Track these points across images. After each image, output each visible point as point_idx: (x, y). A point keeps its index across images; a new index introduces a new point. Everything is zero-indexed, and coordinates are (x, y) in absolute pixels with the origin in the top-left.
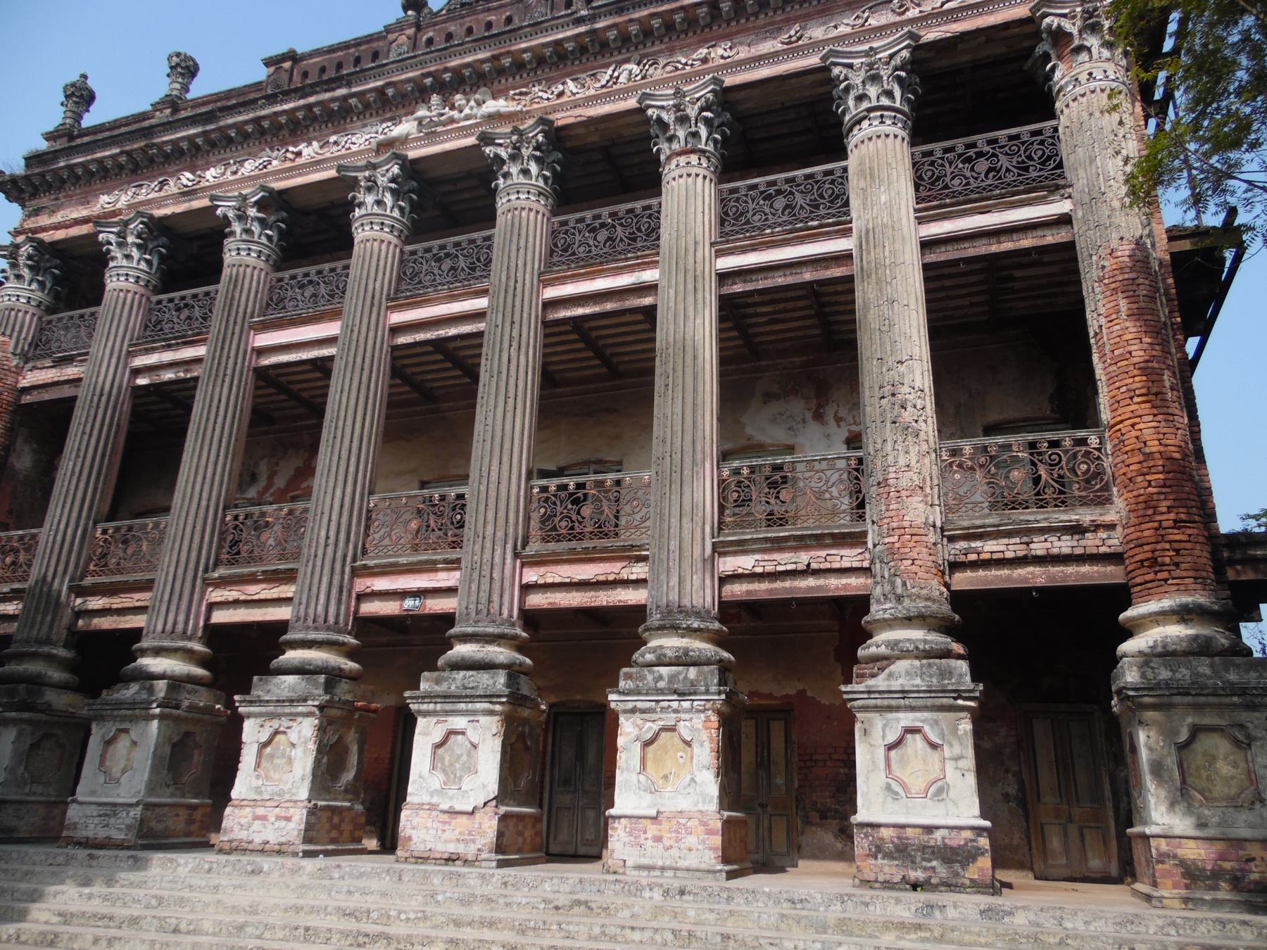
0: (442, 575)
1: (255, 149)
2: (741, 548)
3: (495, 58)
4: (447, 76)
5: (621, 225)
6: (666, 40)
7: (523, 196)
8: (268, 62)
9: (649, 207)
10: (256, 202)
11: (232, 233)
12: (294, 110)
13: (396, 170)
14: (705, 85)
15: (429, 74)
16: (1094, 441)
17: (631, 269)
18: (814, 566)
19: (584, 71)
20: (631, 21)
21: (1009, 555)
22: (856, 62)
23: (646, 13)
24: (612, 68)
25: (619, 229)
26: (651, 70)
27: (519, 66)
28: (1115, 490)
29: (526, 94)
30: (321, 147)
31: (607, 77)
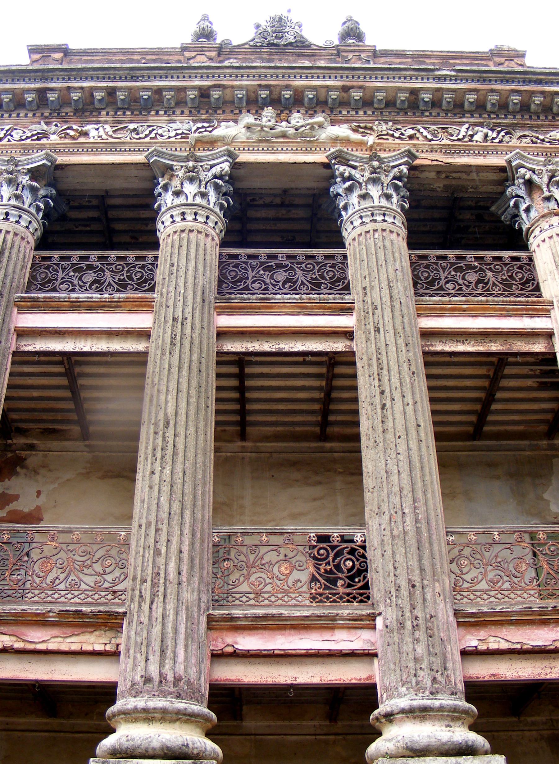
1: (25, 121)
3: (345, 89)
5: (490, 269)
6: (519, 116)
7: (390, 219)
8: (33, 50)
9: (517, 259)
10: (29, 170)
12: (92, 90)
13: (226, 167)
15: (267, 87)
19: (434, 124)
20: (492, 91)
23: (508, 87)
24: (467, 126)
25: (490, 274)
26: (507, 138)
27: (367, 103)
29: (371, 129)
31: (463, 133)
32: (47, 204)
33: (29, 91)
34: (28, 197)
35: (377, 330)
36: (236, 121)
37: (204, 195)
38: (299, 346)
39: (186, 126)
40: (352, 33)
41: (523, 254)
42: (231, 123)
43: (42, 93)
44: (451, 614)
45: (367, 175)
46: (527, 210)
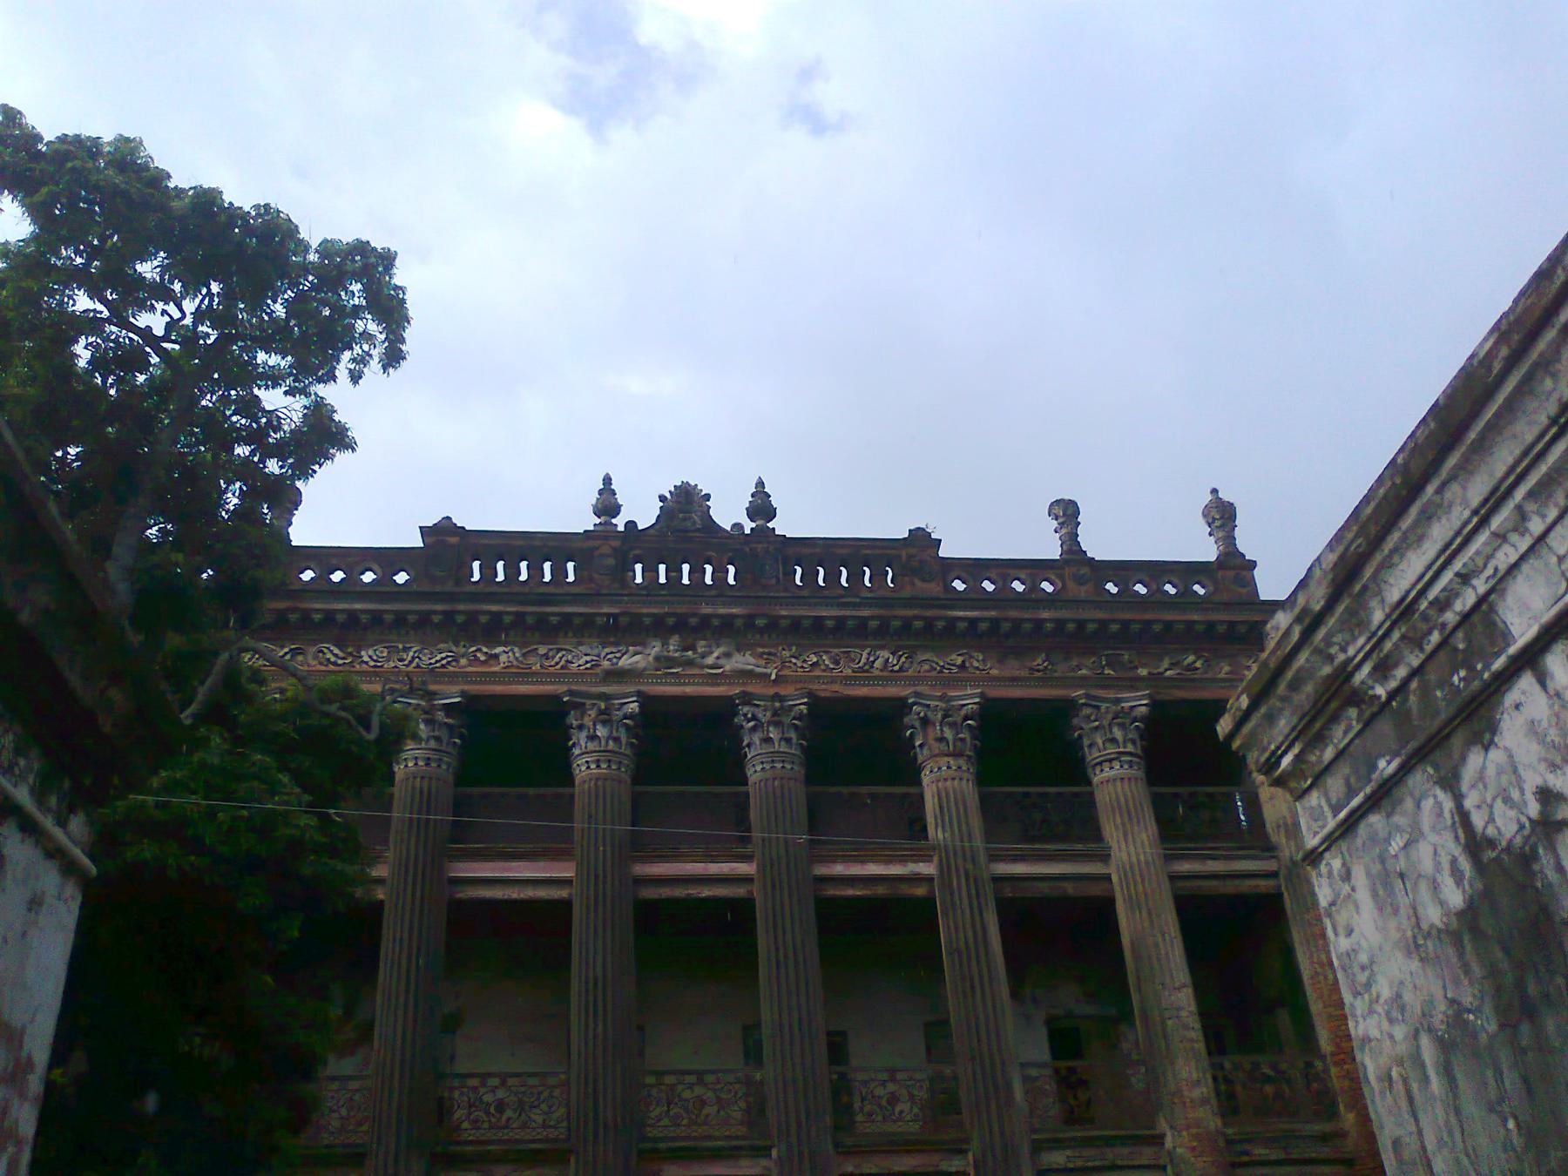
0: (744, 1162)
2: (1057, 1144)
4: (693, 621)
11: (415, 737)
14: (971, 696)
16: (1319, 1064)
17: (903, 860)
18: (1119, 1163)
20: (895, 617)
21: (1273, 1157)
22: (1104, 706)
28: (1342, 1107)
30: (524, 655)
32: (461, 737)
33: (435, 612)
34: (444, 734)
35: (773, 886)
36: (644, 644)
37: (617, 740)
38: (706, 892)
39: (596, 651)
40: (762, 507)
41: (913, 790)
42: (639, 648)
43: (449, 616)
44: (830, 1147)
45: (769, 714)
46: (921, 746)
